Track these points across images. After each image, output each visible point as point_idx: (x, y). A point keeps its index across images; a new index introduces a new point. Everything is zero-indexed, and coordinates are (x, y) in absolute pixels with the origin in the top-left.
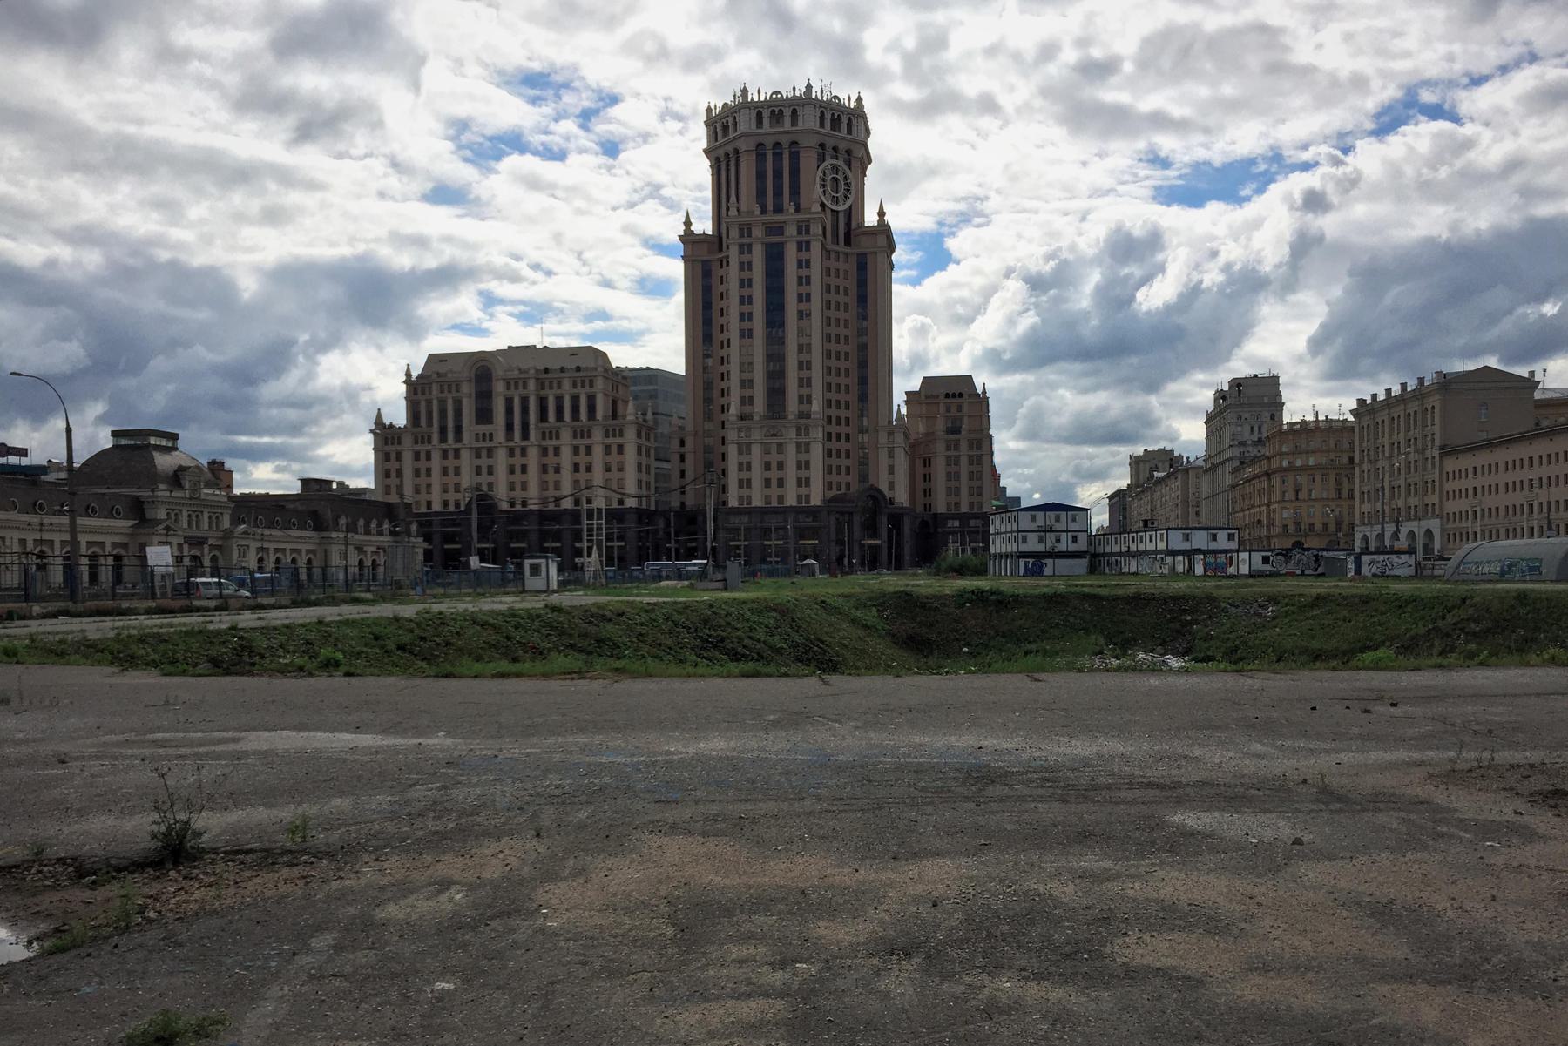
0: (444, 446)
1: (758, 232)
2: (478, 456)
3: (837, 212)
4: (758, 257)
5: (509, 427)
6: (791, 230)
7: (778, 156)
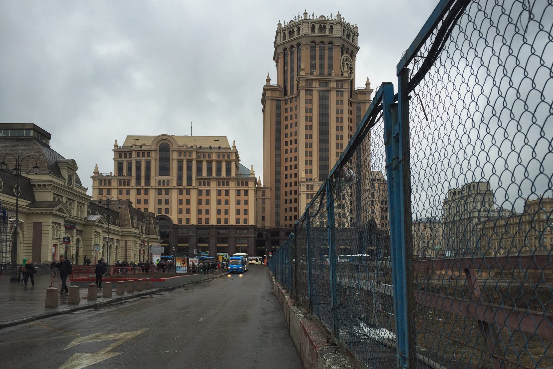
1: (316, 84)
2: (160, 194)
4: (315, 96)
5: (180, 178)
7: (322, 49)
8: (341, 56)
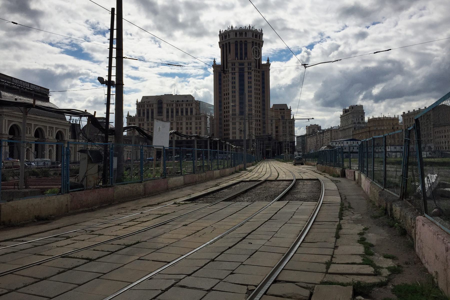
0: (148, 122)
1: (237, 64)
3: (256, 60)
6: (246, 64)
7: (241, 45)
8: (252, 47)
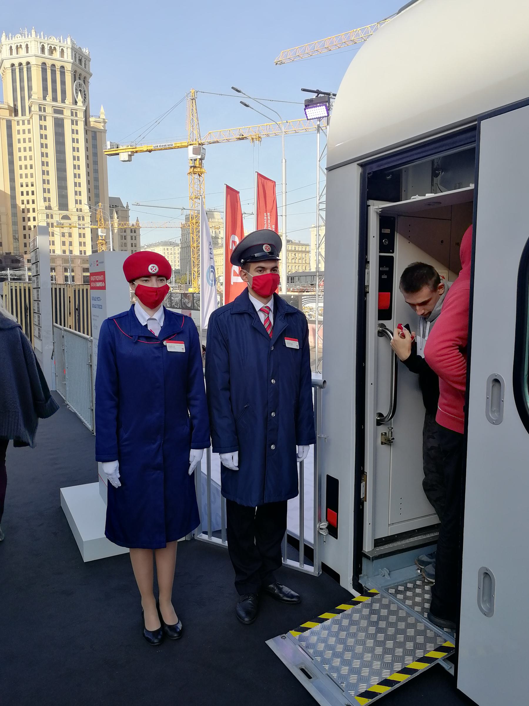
1: (49, 110)
4: (50, 123)
7: (53, 72)
8: (74, 82)
